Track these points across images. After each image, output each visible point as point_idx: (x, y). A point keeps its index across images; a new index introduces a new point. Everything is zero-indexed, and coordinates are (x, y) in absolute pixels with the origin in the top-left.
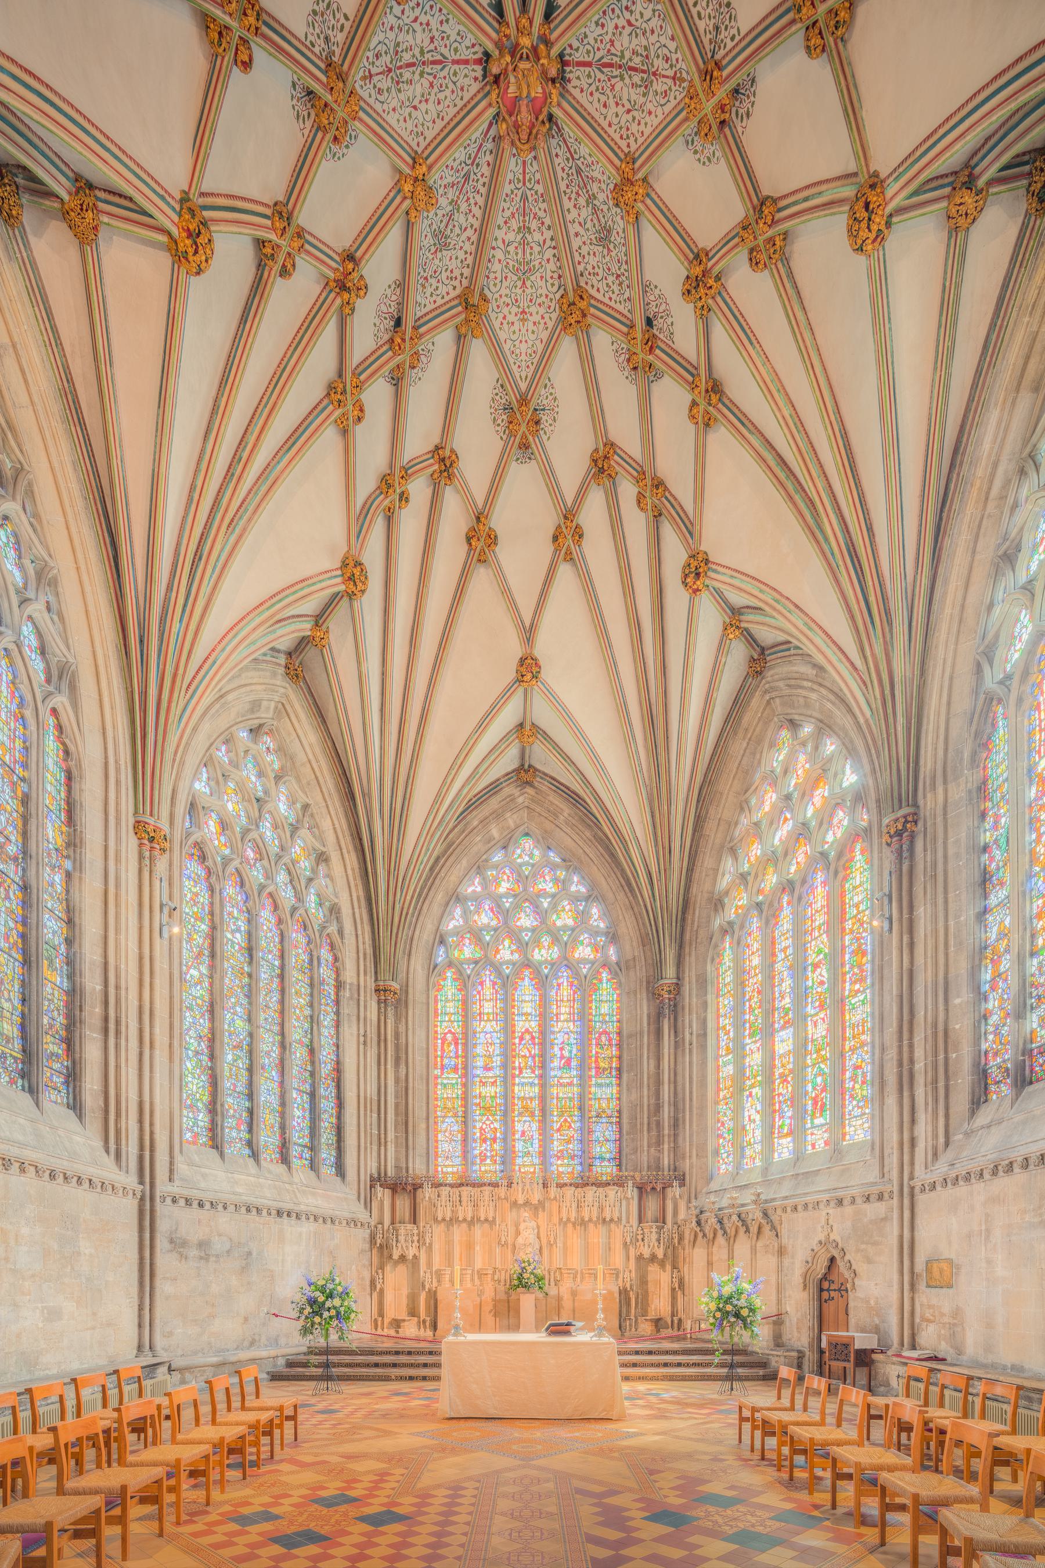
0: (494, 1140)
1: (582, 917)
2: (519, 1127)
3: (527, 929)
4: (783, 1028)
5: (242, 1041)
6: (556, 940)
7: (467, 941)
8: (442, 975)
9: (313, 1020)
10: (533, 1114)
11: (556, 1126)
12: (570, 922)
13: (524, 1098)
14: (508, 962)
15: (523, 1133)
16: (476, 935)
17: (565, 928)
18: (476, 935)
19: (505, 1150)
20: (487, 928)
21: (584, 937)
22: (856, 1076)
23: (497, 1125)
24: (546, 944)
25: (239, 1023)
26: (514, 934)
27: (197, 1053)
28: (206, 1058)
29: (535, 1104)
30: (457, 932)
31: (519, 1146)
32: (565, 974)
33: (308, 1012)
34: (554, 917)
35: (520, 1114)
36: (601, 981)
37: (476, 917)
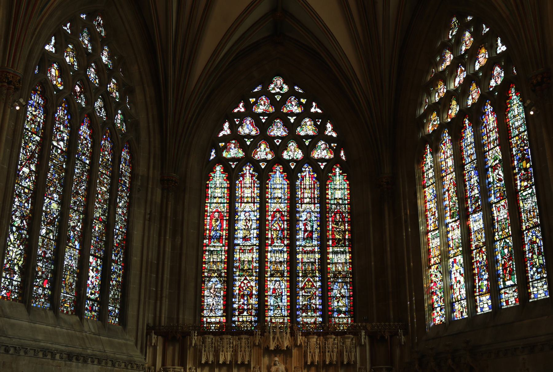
0: (251, 295)
1: (321, 129)
2: (270, 285)
3: (278, 137)
4: (475, 212)
5: (54, 218)
6: (301, 146)
7: (233, 146)
8: (212, 170)
9: (112, 204)
10: (282, 276)
11: (301, 285)
12: (311, 133)
13: (276, 263)
14: (265, 160)
15: (274, 290)
16: (240, 140)
17: (307, 137)
18: (240, 140)
19: (259, 303)
20: (249, 136)
21: (322, 144)
22: (533, 248)
23: (253, 284)
24: (292, 148)
25: (54, 206)
26: (270, 141)
27: (19, 228)
28: (25, 232)
29: (284, 267)
30: (226, 139)
31: (271, 301)
32: (307, 170)
33: (107, 197)
34: (299, 129)
35: (272, 275)
36: (335, 175)
37: (240, 129)
